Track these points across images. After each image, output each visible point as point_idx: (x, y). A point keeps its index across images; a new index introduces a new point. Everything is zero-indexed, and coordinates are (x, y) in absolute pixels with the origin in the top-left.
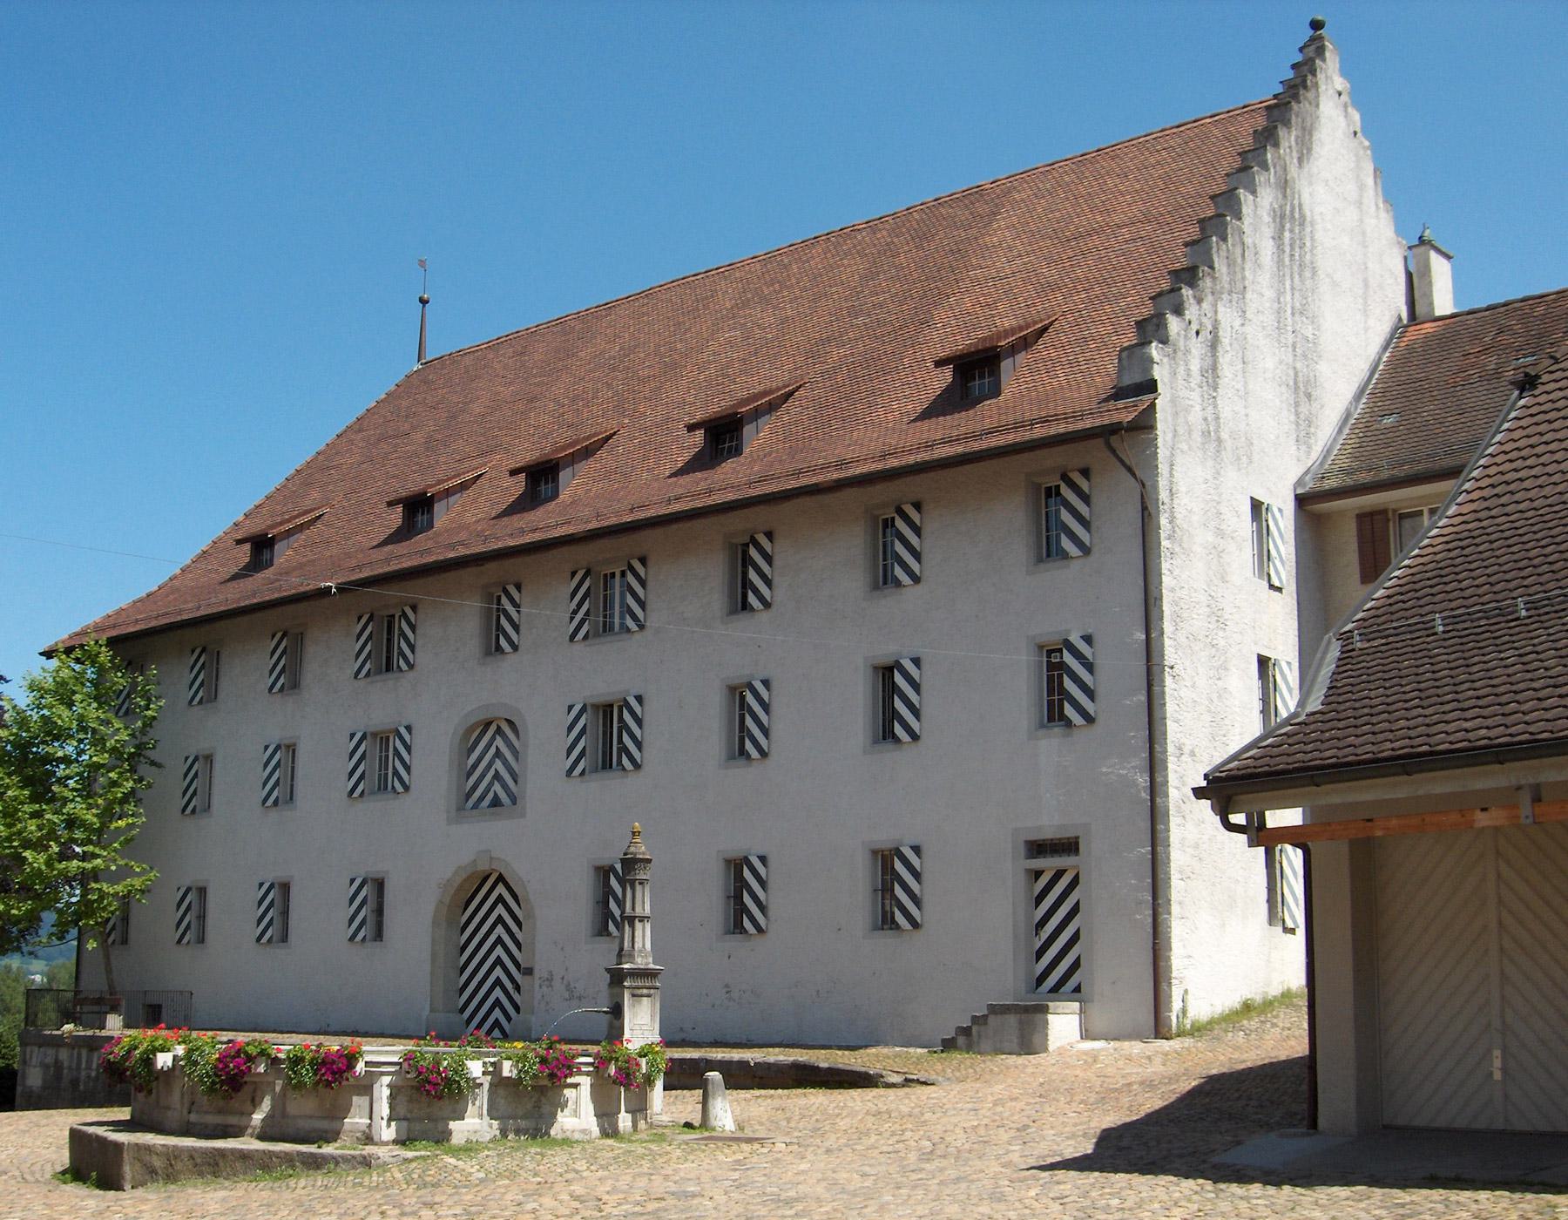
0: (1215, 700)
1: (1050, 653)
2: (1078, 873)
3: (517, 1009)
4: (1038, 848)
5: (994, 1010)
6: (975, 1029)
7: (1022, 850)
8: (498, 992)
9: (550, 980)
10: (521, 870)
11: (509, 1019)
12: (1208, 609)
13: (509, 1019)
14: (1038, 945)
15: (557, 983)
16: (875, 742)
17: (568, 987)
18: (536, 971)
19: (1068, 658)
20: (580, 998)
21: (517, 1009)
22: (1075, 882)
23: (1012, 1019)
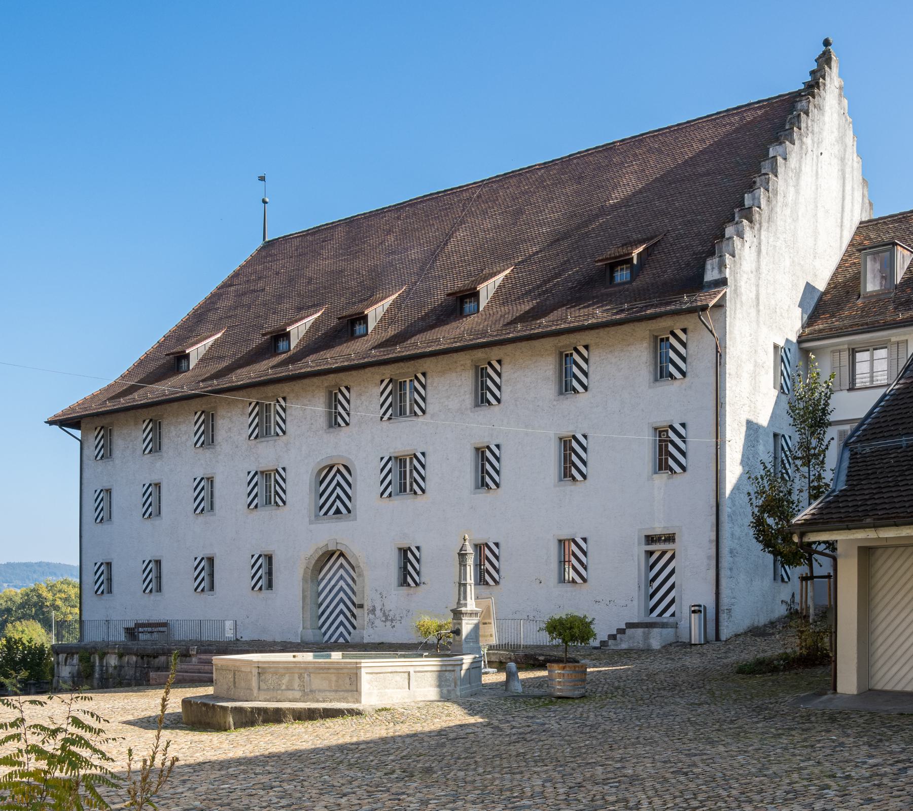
0: (751, 459)
1: (660, 432)
2: (674, 553)
3: (354, 628)
4: (651, 539)
5: (630, 625)
6: (618, 636)
7: (643, 539)
8: (341, 617)
9: (373, 611)
10: (356, 549)
11: (350, 633)
12: (748, 408)
13: (350, 633)
14: (651, 591)
15: (378, 612)
16: (560, 480)
17: (384, 614)
18: (366, 607)
19: (671, 434)
20: (392, 621)
21: (354, 628)
22: (673, 557)
23: (640, 631)
